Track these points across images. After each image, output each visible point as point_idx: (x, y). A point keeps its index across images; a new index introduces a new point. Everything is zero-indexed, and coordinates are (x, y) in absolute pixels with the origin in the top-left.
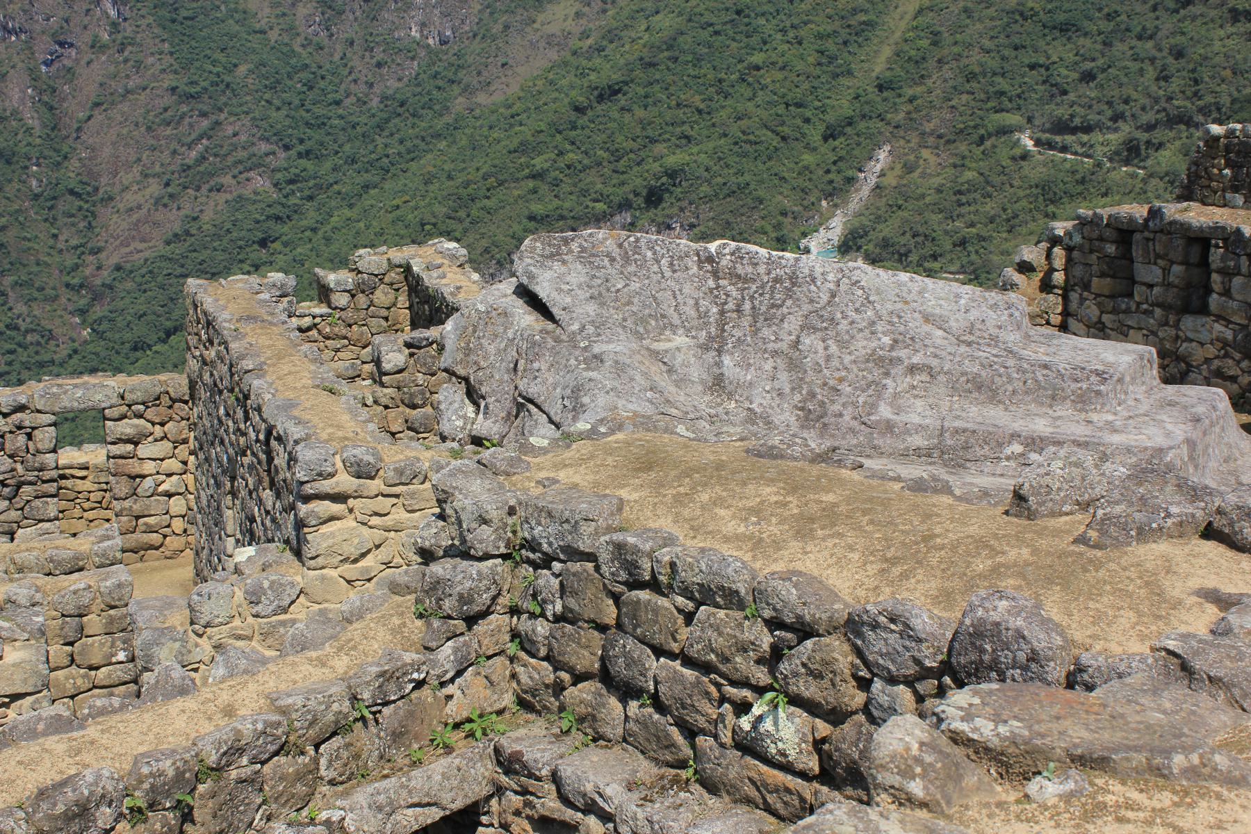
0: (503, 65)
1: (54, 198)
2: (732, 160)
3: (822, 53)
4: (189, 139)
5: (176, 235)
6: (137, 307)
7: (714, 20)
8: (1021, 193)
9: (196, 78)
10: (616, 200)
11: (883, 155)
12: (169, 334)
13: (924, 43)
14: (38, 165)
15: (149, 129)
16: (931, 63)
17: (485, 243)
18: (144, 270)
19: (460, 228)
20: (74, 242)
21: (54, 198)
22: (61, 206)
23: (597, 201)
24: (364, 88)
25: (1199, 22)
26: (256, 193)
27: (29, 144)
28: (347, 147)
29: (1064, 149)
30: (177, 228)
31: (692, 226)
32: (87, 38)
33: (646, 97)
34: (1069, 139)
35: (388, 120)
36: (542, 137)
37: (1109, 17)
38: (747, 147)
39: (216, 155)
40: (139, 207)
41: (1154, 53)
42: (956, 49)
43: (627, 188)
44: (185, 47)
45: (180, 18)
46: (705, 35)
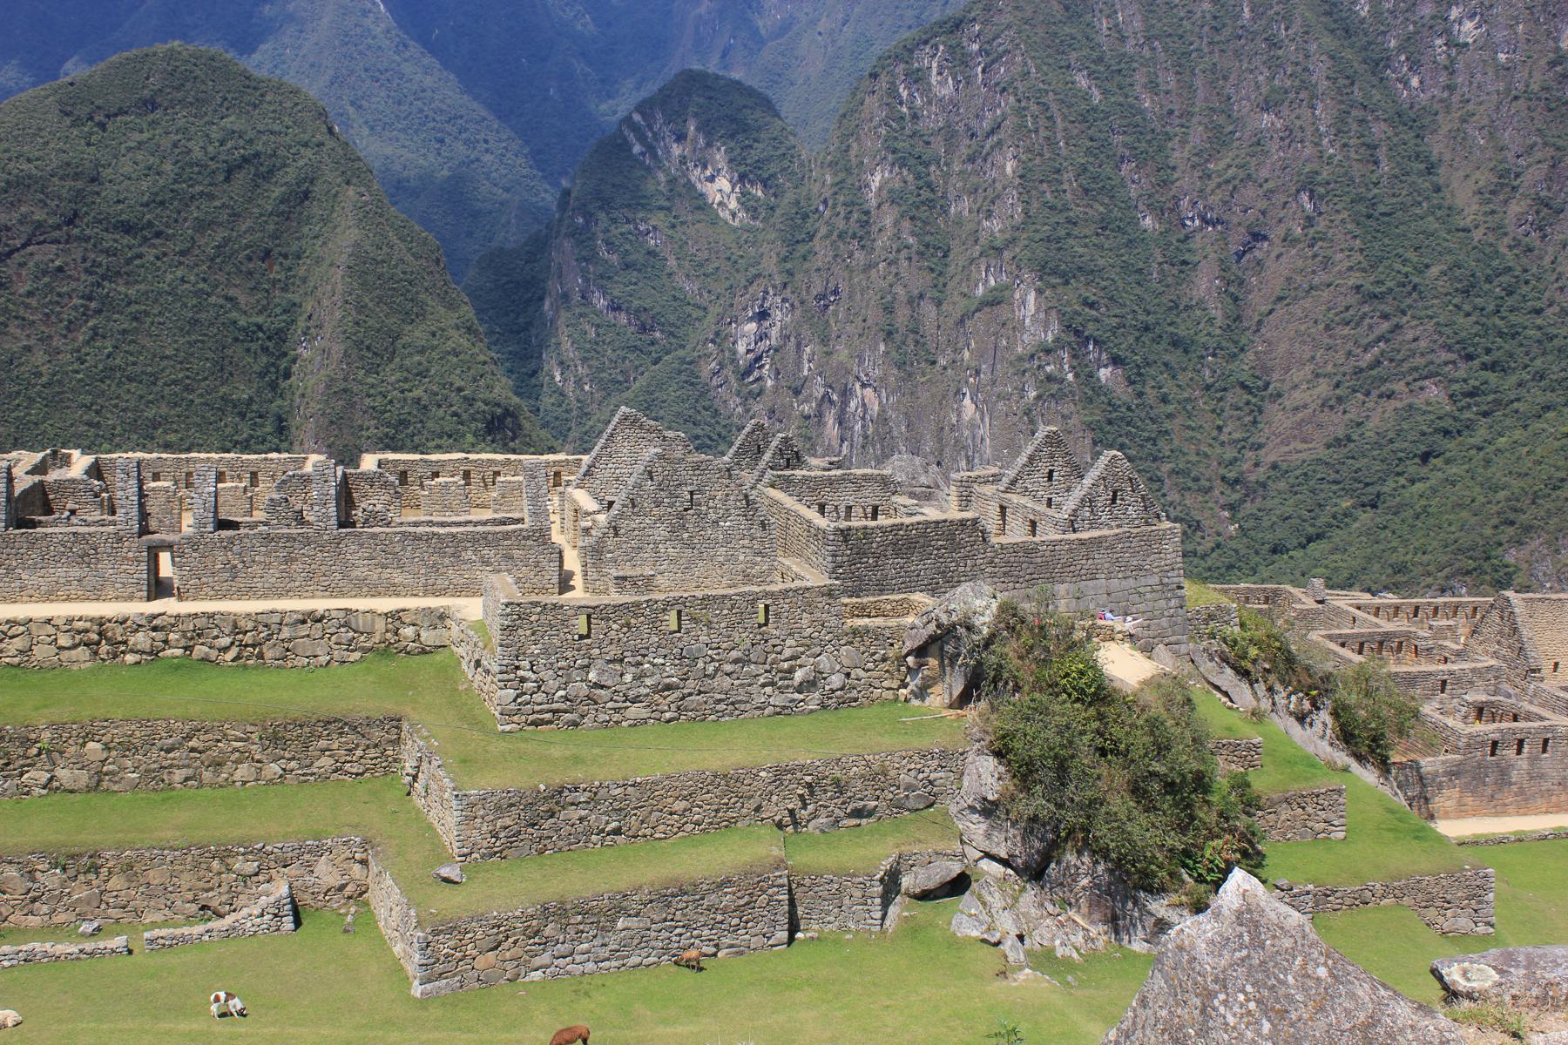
1: (1225, 389)
4: (1366, 341)
5: (1337, 440)
6: (1284, 509)
12: (1310, 540)
14: (1214, 355)
15: (1327, 328)
18: (1298, 472)
20: (1236, 436)
21: (1225, 389)
22: (1231, 397)
26: (1428, 404)
28: (1538, 362)
30: (1340, 434)
32: (1280, 231)
39: (1392, 360)
40: (1305, 406)
44: (1376, 245)
45: (1376, 214)
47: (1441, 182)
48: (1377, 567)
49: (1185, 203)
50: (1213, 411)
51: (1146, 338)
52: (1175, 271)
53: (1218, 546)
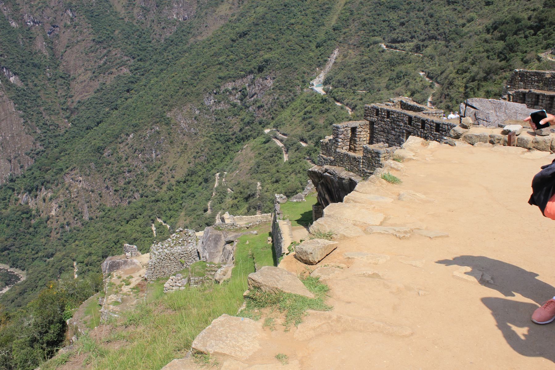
2: (286, 55)
3: (314, 18)
4: (100, 57)
5: (98, 90)
7: (277, 9)
8: (383, 63)
9: (101, 36)
10: (248, 71)
11: (336, 52)
12: (98, 123)
13: (348, 14)
15: (86, 54)
16: (351, 21)
17: (204, 87)
18: (88, 102)
20: (63, 94)
22: (58, 82)
23: (242, 71)
24: (158, 36)
25: (437, 5)
26: (124, 74)
27: (45, 61)
28: (154, 57)
29: (396, 48)
30: (98, 88)
31: (274, 78)
32: (63, 24)
34: (397, 45)
35: (167, 47)
37: (408, 4)
38: (291, 51)
39: (110, 62)
40: (85, 81)
41: (423, 15)
42: (358, 16)
43: (251, 67)
44: (97, 25)
46: (274, 14)
48: (127, 127)
49: (26, 17)
50: (53, 87)
51: (24, 65)
52: (28, 41)
53: (67, 131)
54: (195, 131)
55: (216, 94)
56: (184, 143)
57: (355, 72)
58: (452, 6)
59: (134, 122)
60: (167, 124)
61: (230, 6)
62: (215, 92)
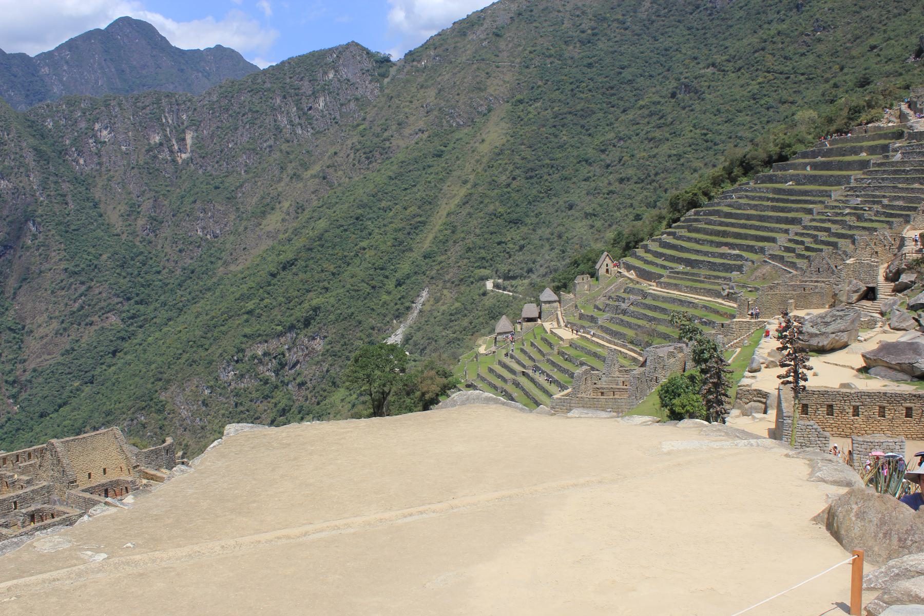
0: (244, 249)
5: (67, 351)
7: (344, 223)
10: (288, 324)
11: (424, 294)
12: (60, 406)
13: (448, 232)
15: (53, 292)
16: (451, 242)
17: (220, 351)
18: (48, 371)
19: (208, 342)
20: (10, 357)
24: (173, 264)
25: (572, 218)
26: (112, 325)
28: (162, 297)
31: (325, 337)
33: (306, 267)
35: (185, 281)
36: (252, 291)
37: (537, 216)
38: (353, 293)
39: (89, 305)
40: (47, 336)
42: (462, 235)
43: (292, 318)
44: (73, 246)
46: (338, 231)
47: (102, 211)
53: (9, 419)
54: (201, 424)
55: (237, 362)
56: (184, 443)
57: (438, 329)
58: (589, 222)
59: (108, 407)
60: (159, 411)
61: (283, 216)
62: (235, 358)
